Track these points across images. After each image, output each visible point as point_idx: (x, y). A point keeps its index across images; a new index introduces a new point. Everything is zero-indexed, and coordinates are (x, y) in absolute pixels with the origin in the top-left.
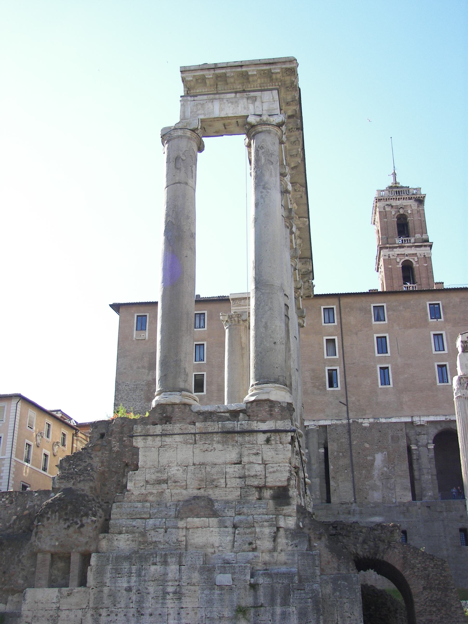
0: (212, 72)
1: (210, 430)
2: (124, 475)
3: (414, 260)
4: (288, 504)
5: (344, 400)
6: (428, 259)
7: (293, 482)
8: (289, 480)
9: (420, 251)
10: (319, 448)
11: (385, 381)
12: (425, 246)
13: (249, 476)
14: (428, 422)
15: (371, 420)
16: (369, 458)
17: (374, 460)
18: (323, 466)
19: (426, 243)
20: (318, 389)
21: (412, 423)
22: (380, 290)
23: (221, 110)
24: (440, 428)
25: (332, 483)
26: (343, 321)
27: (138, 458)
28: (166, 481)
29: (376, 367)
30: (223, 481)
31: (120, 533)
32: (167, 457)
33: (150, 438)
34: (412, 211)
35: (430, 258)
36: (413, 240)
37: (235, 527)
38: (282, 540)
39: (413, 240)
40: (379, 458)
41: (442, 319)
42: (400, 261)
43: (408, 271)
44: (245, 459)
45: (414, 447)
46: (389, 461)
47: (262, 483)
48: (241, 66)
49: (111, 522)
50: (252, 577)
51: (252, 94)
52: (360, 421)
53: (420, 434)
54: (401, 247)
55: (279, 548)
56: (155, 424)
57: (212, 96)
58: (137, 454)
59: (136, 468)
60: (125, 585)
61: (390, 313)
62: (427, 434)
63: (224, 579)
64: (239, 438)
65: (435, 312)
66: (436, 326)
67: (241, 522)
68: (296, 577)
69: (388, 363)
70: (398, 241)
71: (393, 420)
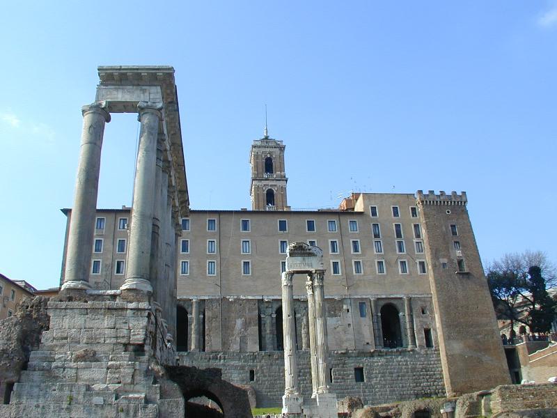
0: (118, 71)
1: (97, 306)
2: (40, 333)
4: (144, 355)
6: (284, 189)
7: (148, 341)
8: (145, 340)
10: (199, 314)
12: (283, 180)
13: (120, 337)
14: (273, 300)
15: (236, 297)
17: (235, 324)
18: (202, 327)
21: (263, 300)
22: (250, 208)
23: (123, 97)
27: (49, 323)
28: (66, 338)
30: (103, 339)
31: (35, 370)
32: (66, 322)
33: (58, 310)
36: (275, 176)
37: (108, 368)
38: (138, 378)
39: (275, 176)
40: (239, 322)
43: (270, 197)
44: (117, 326)
45: (262, 316)
46: (246, 325)
47: (127, 342)
48: (137, 69)
49: (29, 363)
50: (116, 399)
51: (144, 87)
52: (227, 297)
53: (267, 307)
54: (267, 179)
55: (135, 382)
56: (61, 301)
57: (117, 87)
58: (49, 320)
59: (48, 329)
60: (36, 403)
62: (272, 307)
63: (98, 400)
64: (115, 312)
65: (283, 226)
66: (281, 236)
67: (113, 365)
68: (143, 401)
69: (249, 259)
70: (265, 176)
71: (250, 298)
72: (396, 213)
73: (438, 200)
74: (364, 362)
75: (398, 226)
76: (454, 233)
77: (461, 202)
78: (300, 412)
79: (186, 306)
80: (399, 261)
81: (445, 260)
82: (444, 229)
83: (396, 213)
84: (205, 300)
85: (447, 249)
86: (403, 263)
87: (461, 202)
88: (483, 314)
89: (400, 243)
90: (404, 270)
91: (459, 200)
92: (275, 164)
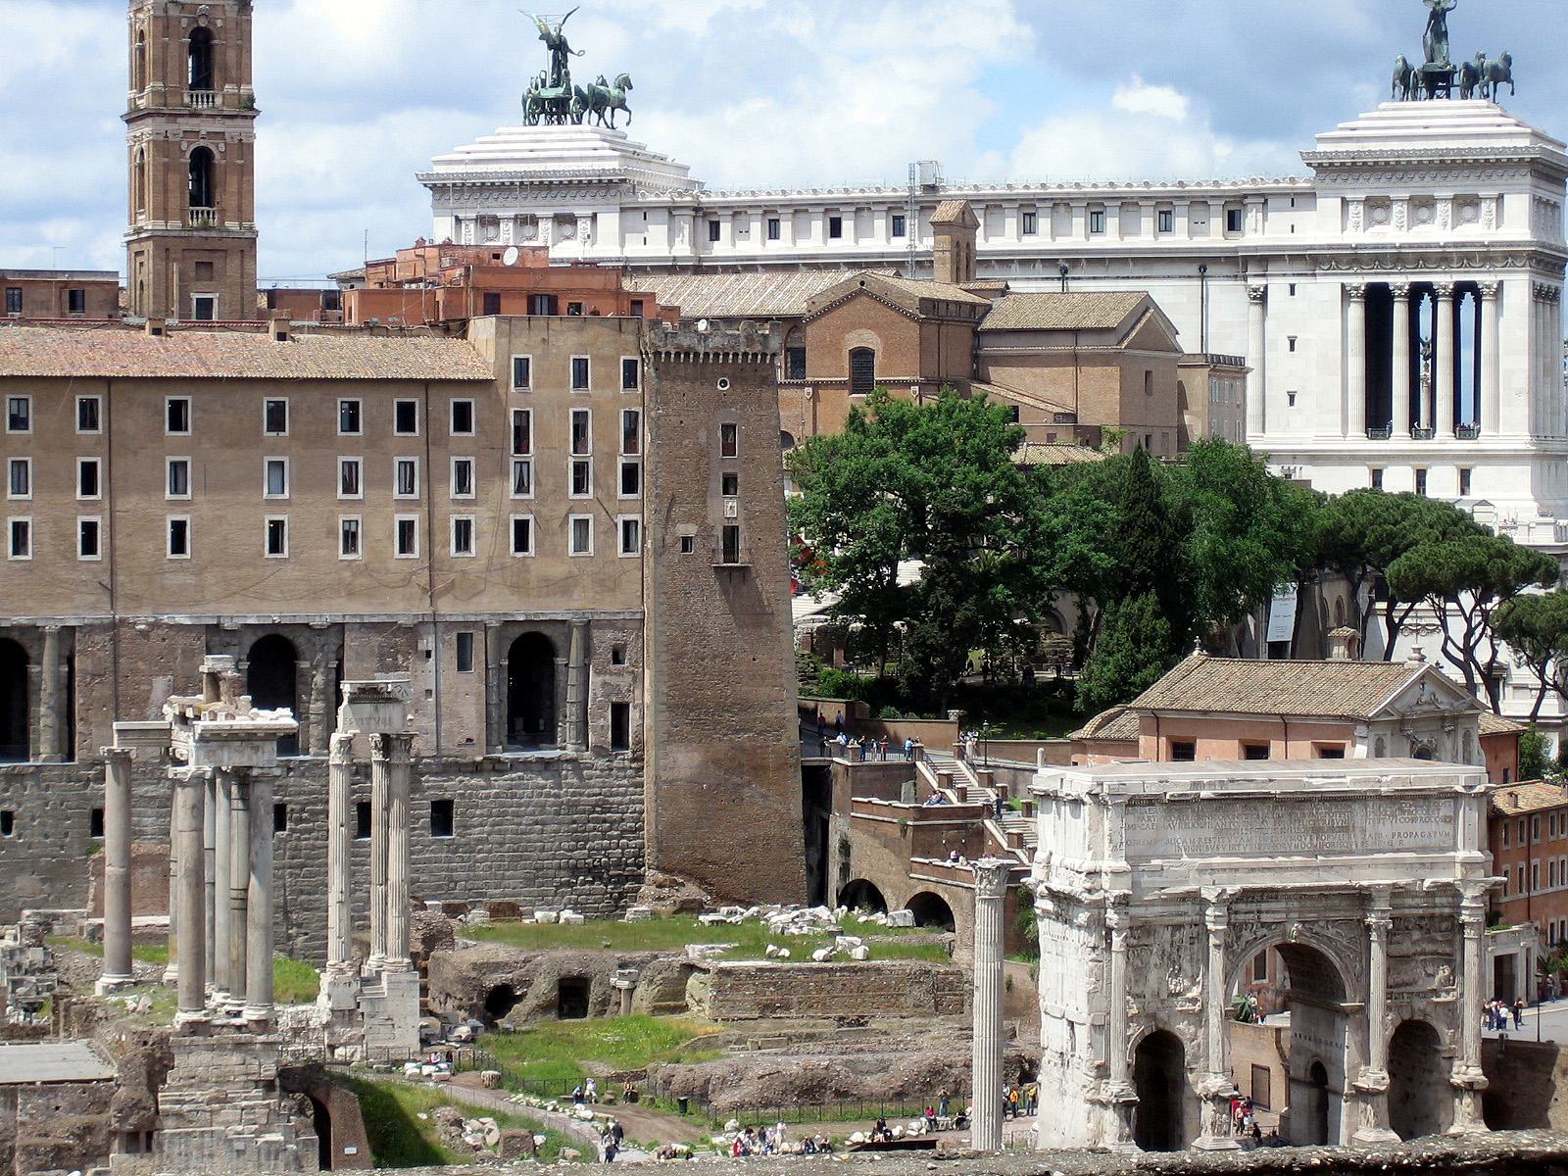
3: (217, 149)
5: (106, 581)
9: (232, 129)
10: (60, 664)
11: (179, 546)
16: (142, 687)
17: (150, 691)
18: (65, 696)
19: (247, 109)
20: (65, 557)
24: (261, 634)
25: (79, 727)
26: (114, 427)
29: (164, 520)
34: (225, 20)
35: (251, 146)
39: (218, 101)
41: (287, 433)
42: (188, 148)
61: (199, 414)
65: (276, 420)
72: (581, 380)
73: (701, 350)
74: (453, 787)
75: (580, 419)
76: (728, 449)
77: (764, 355)
78: (353, 1007)
79: (25, 641)
80: (572, 518)
81: (691, 530)
82: (703, 435)
83: (581, 380)
84: (73, 628)
85: (703, 496)
86: (581, 525)
87: (764, 355)
88: (763, 678)
89: (580, 469)
90: (581, 545)
91: (758, 348)
92: (224, 52)
